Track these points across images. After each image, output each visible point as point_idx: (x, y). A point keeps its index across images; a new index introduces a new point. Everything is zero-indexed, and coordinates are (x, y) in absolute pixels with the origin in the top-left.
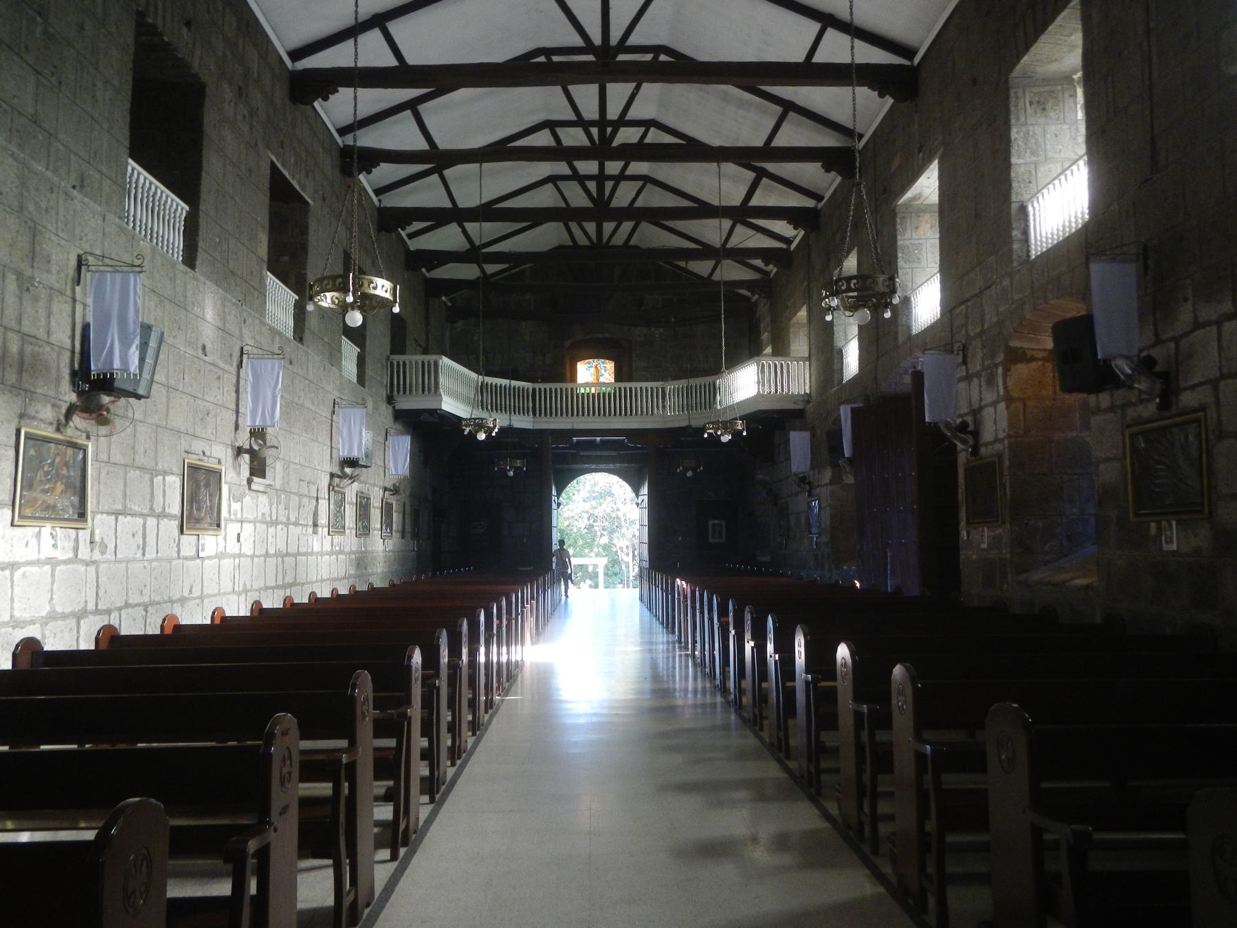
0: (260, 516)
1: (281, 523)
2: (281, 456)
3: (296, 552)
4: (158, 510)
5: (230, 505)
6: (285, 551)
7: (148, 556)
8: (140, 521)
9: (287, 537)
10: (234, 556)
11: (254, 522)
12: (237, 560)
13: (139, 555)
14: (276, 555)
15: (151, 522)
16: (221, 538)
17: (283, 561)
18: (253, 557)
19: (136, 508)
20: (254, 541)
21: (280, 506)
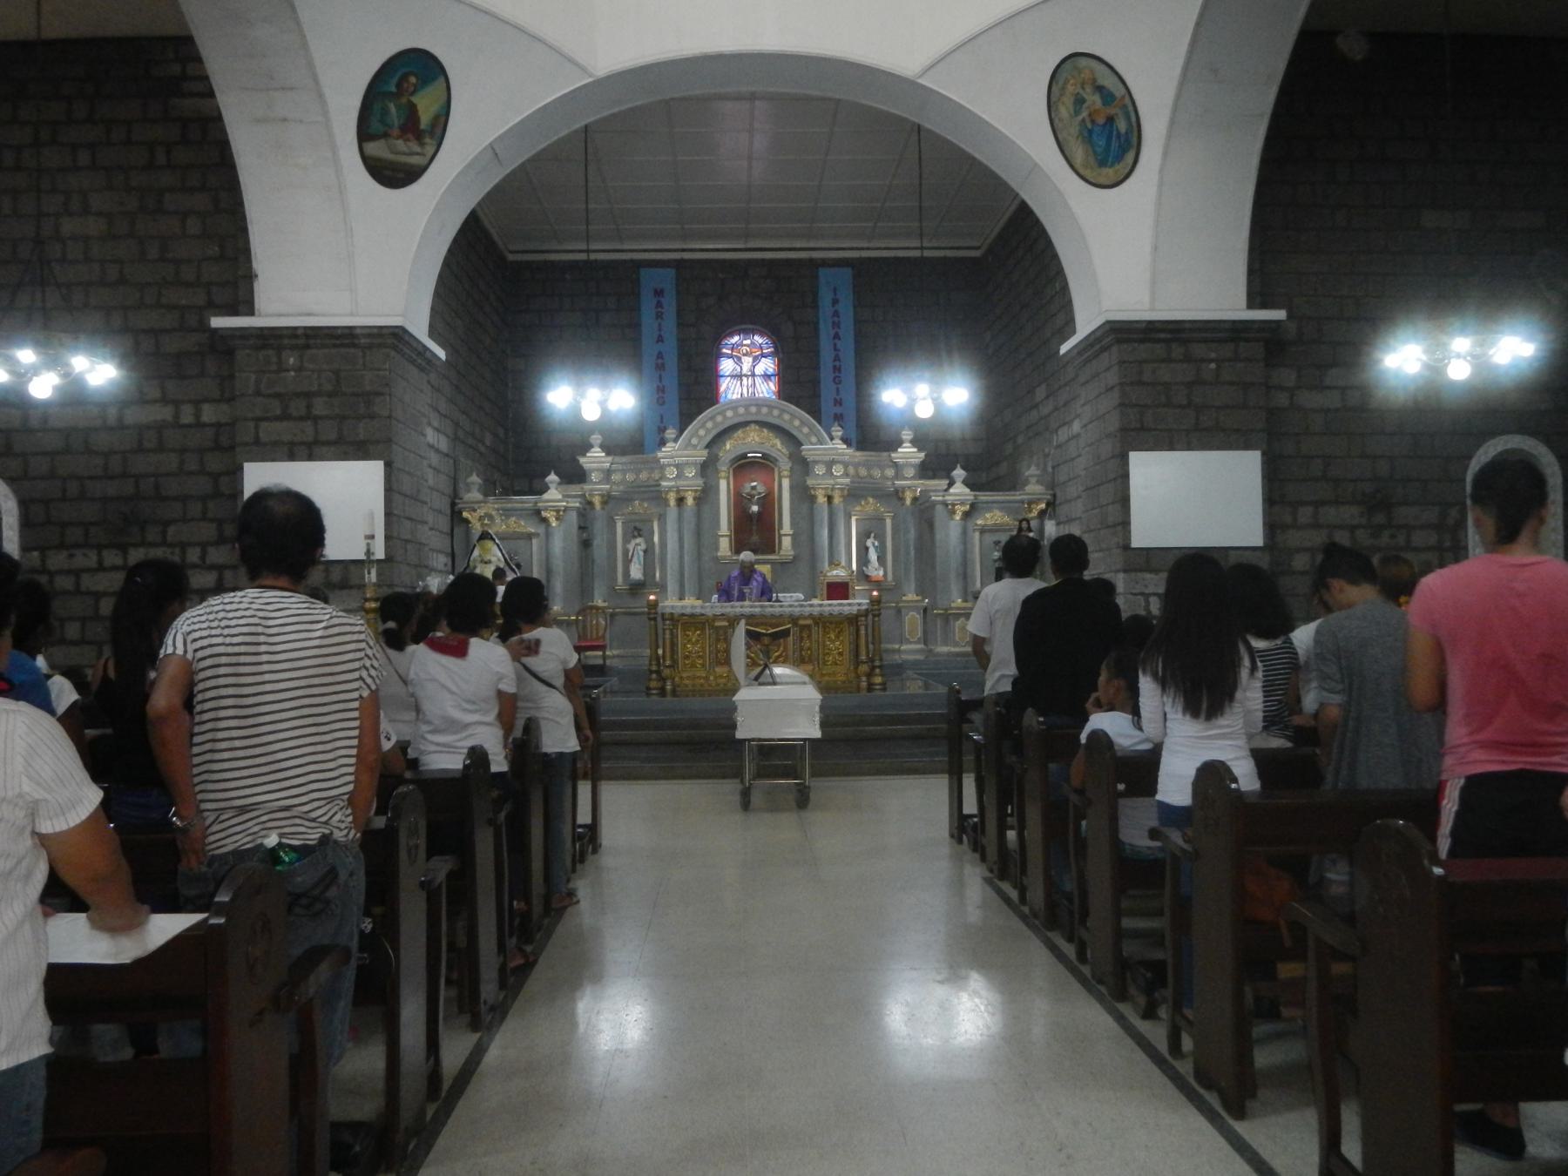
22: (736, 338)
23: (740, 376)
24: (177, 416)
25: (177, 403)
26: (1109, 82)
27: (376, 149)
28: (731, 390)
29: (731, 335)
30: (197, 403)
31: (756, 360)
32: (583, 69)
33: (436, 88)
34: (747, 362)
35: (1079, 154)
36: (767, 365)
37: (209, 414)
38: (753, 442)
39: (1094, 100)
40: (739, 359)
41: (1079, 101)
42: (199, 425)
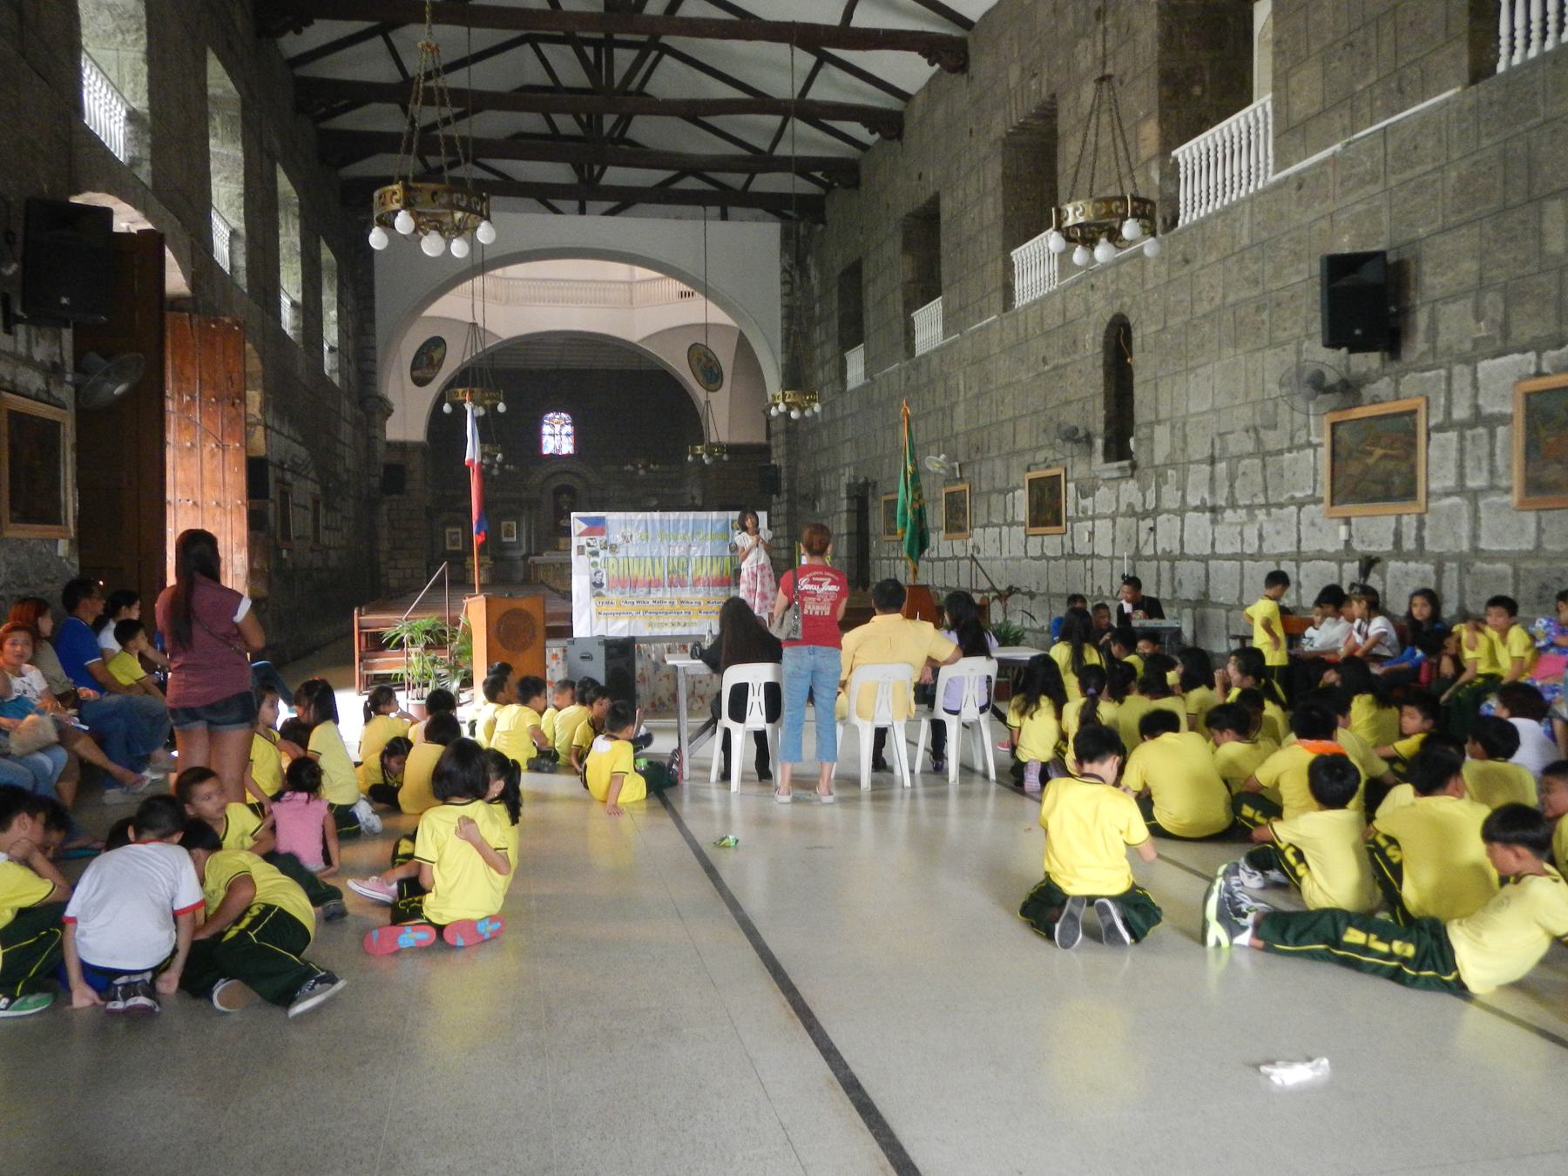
0: (1123, 508)
1: (1168, 511)
2: (1163, 414)
3: (1208, 551)
4: (1009, 519)
5: (1077, 504)
6: (1177, 552)
7: (1004, 555)
8: (997, 530)
9: (1182, 530)
10: (1084, 557)
11: (1113, 518)
12: (1089, 563)
13: (998, 555)
14: (1155, 557)
15: (1005, 529)
16: (1067, 538)
17: (1173, 568)
18: (1112, 559)
19: (995, 521)
20: (1113, 540)
21: (1164, 489)
22: (551, 415)
23: (553, 435)
26: (709, 355)
27: (417, 373)
33: (440, 350)
34: (558, 427)
35: (701, 378)
36: (569, 429)
38: (565, 480)
39: (704, 359)
41: (699, 360)
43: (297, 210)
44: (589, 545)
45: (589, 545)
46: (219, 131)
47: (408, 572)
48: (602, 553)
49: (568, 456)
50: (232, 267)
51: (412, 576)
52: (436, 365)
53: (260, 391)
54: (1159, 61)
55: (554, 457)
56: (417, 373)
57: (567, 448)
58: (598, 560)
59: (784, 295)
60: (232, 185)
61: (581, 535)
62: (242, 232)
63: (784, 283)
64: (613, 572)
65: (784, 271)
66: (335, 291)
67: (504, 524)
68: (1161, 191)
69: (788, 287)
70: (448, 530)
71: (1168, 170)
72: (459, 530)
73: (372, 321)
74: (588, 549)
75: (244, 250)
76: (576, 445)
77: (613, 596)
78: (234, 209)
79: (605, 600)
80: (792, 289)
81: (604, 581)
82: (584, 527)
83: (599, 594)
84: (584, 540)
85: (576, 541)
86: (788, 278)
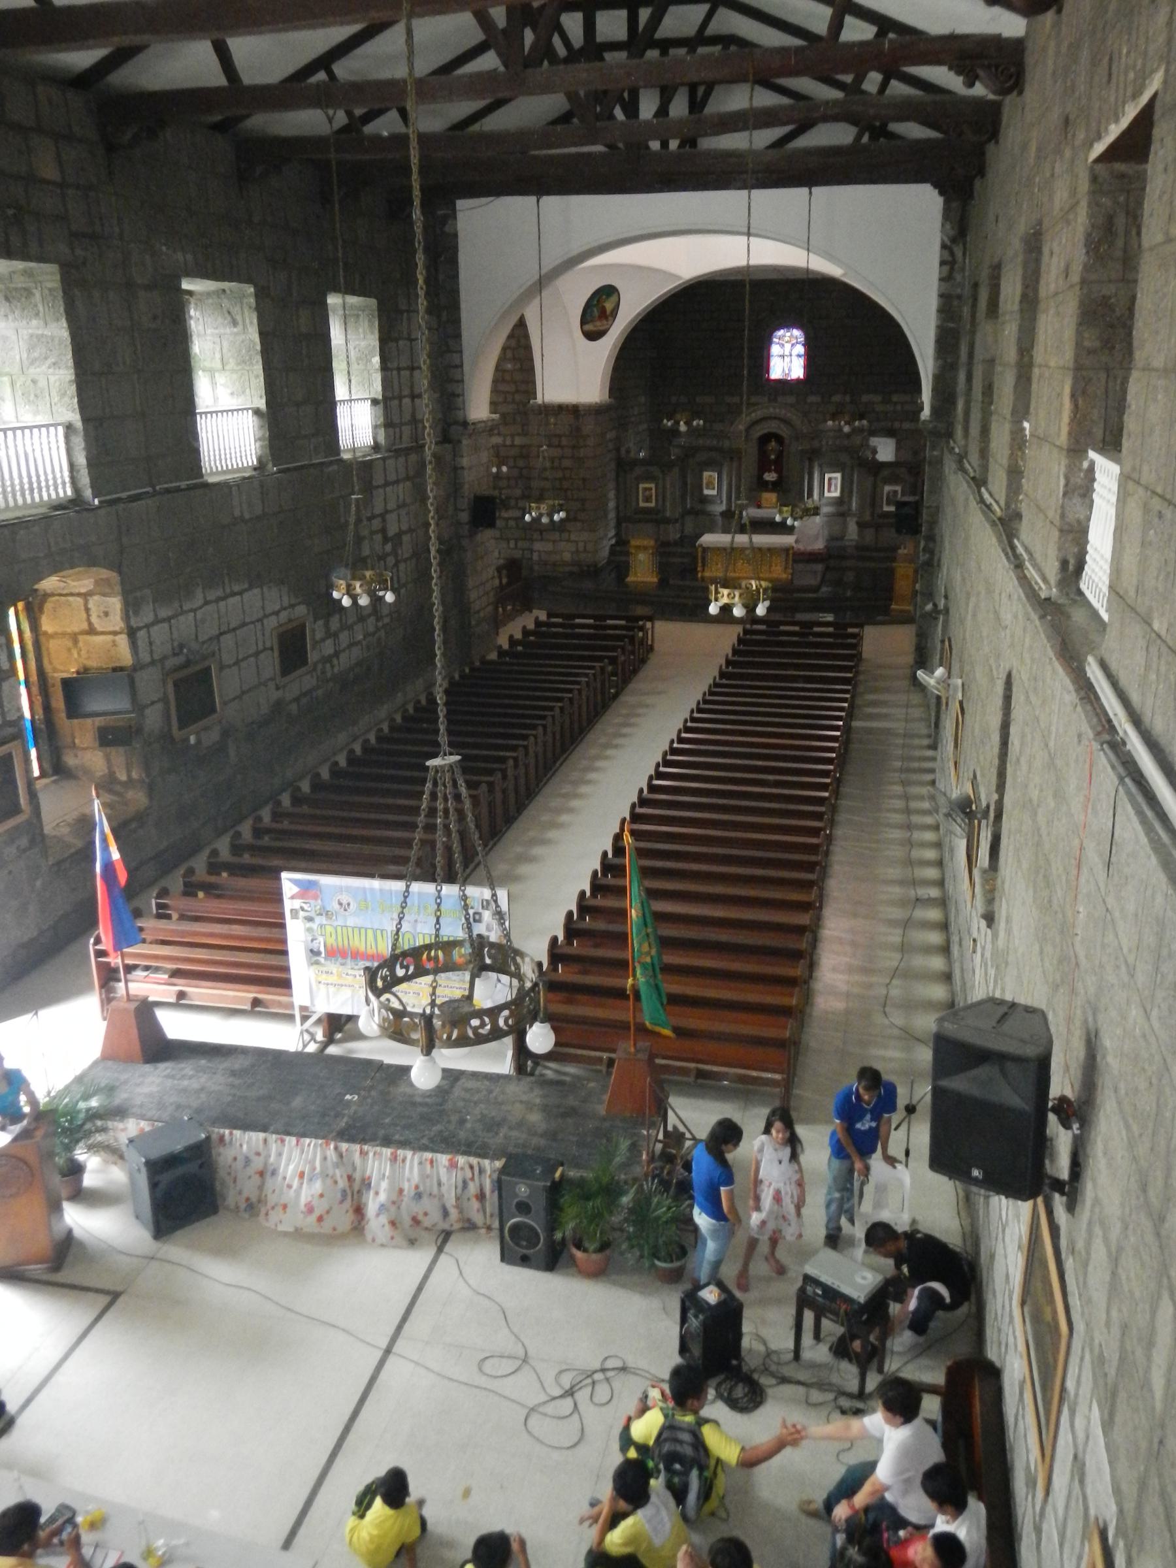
22: (781, 332)
23: (783, 356)
24: (504, 441)
25: (505, 436)
27: (588, 327)
28: (777, 370)
29: (779, 329)
30: (512, 436)
31: (793, 345)
32: (679, 278)
33: (614, 298)
34: (788, 346)
36: (800, 349)
37: (518, 441)
40: (782, 346)
42: (512, 446)
43: (252, 300)
44: (302, 909)
45: (302, 909)
46: (41, 309)
47: (581, 545)
48: (318, 920)
49: (798, 380)
50: (72, 466)
51: (585, 551)
52: (609, 316)
53: (119, 598)
54: (1083, 282)
55: (784, 385)
56: (588, 327)
57: (797, 371)
58: (314, 926)
59: (941, 280)
60: (61, 372)
61: (292, 897)
62: (79, 424)
63: (943, 263)
64: (331, 941)
65: (944, 246)
66: (377, 335)
67: (706, 474)
68: (1063, 516)
69: (946, 268)
70: (641, 486)
71: (1079, 479)
72: (653, 486)
73: (458, 336)
74: (302, 914)
75: (83, 445)
76: (808, 367)
77: (333, 967)
78: (66, 399)
79: (325, 969)
80: (952, 270)
81: (322, 949)
82: (295, 890)
83: (317, 963)
84: (297, 904)
85: (289, 905)
86: (948, 257)
